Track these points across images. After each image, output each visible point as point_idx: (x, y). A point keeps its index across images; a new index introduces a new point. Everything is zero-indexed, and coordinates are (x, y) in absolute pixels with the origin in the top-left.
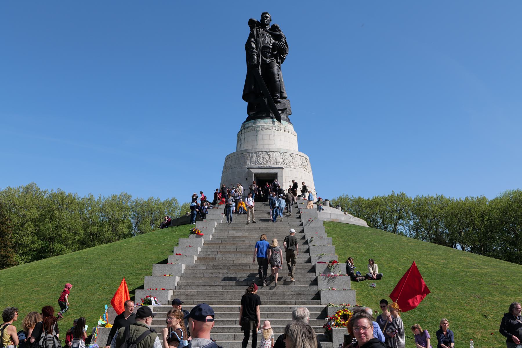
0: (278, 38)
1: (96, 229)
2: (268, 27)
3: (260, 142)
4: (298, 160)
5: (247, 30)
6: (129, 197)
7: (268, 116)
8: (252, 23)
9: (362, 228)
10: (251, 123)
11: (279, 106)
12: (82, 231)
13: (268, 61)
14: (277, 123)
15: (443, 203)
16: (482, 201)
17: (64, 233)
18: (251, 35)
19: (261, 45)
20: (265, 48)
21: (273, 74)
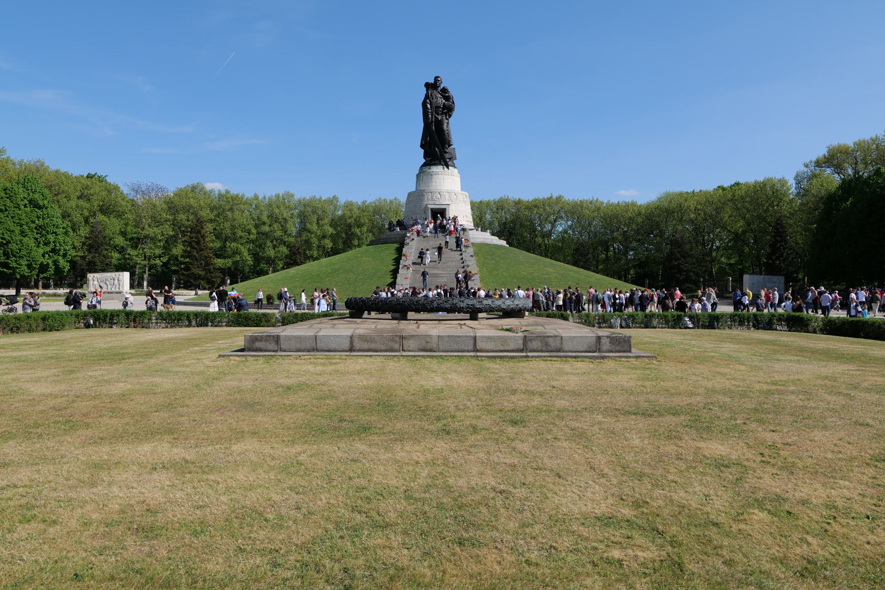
0: (447, 98)
1: (266, 228)
2: (439, 89)
3: (434, 184)
4: (461, 198)
5: (423, 91)
6: (292, 196)
7: (440, 164)
8: (427, 85)
9: (501, 246)
10: (426, 169)
11: (447, 156)
12: (254, 231)
13: (440, 118)
14: (446, 169)
15: (597, 207)
16: (634, 204)
17: (239, 233)
18: (427, 97)
19: (434, 106)
20: (438, 107)
21: (443, 131)
